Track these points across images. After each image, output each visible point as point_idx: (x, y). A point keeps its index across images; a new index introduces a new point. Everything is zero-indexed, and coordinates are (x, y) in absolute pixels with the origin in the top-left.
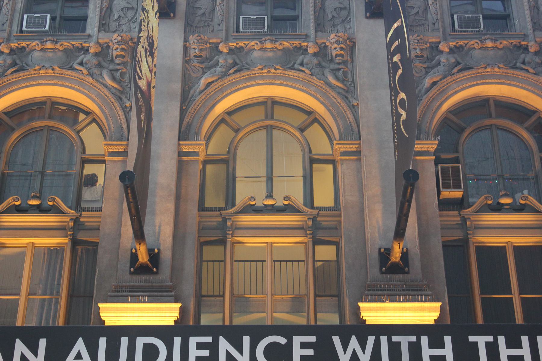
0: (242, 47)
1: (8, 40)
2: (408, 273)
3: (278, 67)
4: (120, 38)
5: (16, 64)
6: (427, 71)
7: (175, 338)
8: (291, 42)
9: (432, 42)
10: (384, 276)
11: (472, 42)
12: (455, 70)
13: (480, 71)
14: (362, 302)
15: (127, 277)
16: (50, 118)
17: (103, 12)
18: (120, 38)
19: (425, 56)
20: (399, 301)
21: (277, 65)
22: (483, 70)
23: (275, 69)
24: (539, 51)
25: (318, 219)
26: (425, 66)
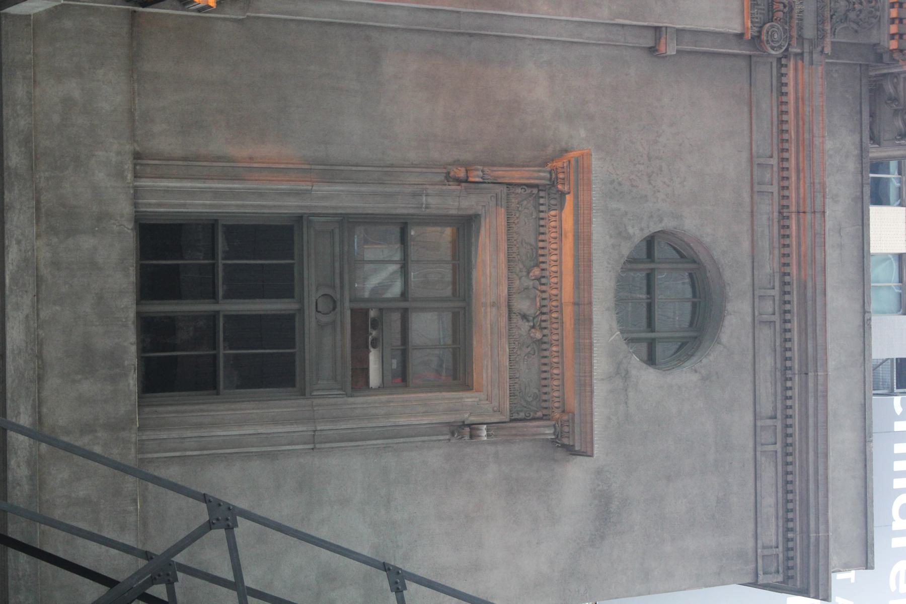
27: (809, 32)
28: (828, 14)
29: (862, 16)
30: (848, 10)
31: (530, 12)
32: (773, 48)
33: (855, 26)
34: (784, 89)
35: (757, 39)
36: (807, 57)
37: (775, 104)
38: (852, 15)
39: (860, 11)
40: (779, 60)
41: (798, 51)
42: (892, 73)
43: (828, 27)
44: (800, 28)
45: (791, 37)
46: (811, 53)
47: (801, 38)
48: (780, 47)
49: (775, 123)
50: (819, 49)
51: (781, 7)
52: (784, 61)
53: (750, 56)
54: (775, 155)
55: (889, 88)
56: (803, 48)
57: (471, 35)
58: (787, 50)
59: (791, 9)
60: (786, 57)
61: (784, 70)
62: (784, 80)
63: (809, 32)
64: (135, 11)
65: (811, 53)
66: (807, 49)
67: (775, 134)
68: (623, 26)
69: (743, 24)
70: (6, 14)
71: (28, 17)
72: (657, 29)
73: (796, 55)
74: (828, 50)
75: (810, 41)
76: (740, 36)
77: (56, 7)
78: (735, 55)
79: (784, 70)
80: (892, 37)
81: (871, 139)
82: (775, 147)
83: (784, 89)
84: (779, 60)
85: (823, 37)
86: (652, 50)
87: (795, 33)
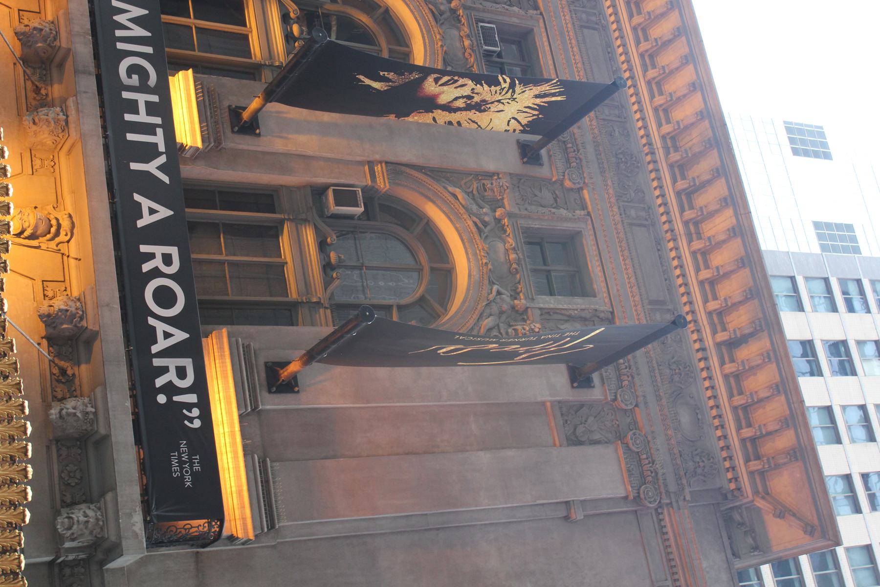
0: (505, 231)
1: (465, 7)
2: (233, 132)
3: (445, 48)
4: (537, 330)
5: (485, 227)
6: (470, 194)
7: (195, 396)
8: (475, 66)
9: (503, 203)
10: (227, 110)
11: (466, 29)
12: (475, 219)
13: (435, 29)
14: (194, 72)
15: (226, 104)
16: (432, 269)
17: (563, 312)
18: (537, 330)
19: (486, 194)
20: (201, 128)
21: (492, 265)
22: (480, 247)
23: (442, 46)
24: (517, 311)
25: (322, 310)
26: (475, 192)
27: (672, 488)
28: (682, 473)
29: (706, 470)
30: (695, 468)
31: (476, 506)
32: (650, 502)
33: (702, 478)
34: (664, 530)
35: (637, 499)
36: (675, 504)
37: (660, 541)
38: (699, 471)
39: (704, 467)
40: (656, 510)
41: (668, 501)
42: (736, 507)
43: (684, 482)
44: (666, 486)
45: (661, 493)
46: (677, 501)
47: (667, 492)
48: (655, 501)
49: (664, 555)
50: (682, 498)
51: (649, 473)
52: (660, 510)
53: (636, 511)
54: (669, 577)
55: (737, 517)
56: (670, 499)
57: (438, 529)
58: (660, 502)
59: (657, 474)
60: (660, 507)
61: (661, 517)
62: (663, 523)
63: (672, 488)
64: (198, 552)
65: (677, 501)
66: (673, 500)
67: (665, 563)
68: (543, 505)
69: (626, 489)
70: (107, 569)
71: (122, 569)
72: (567, 503)
73: (667, 504)
74: (688, 497)
75: (675, 493)
76: (626, 498)
77: (142, 558)
78: (626, 512)
79: (661, 517)
80: (730, 481)
81: (733, 555)
82: (667, 572)
83: (664, 530)
84: (656, 510)
85: (683, 489)
86: (567, 518)
87: (663, 490)
